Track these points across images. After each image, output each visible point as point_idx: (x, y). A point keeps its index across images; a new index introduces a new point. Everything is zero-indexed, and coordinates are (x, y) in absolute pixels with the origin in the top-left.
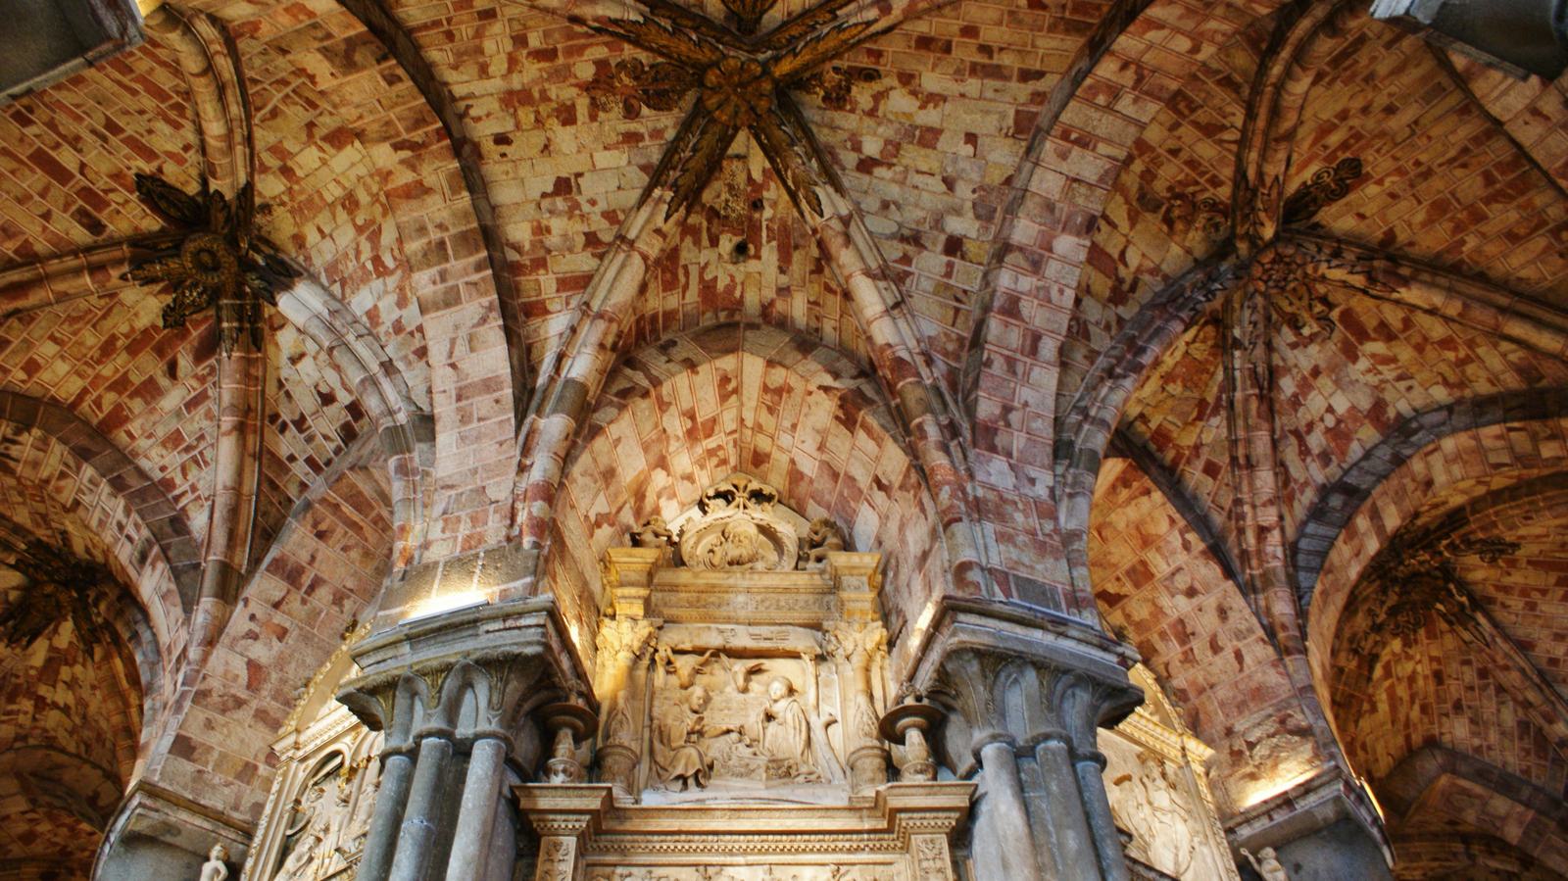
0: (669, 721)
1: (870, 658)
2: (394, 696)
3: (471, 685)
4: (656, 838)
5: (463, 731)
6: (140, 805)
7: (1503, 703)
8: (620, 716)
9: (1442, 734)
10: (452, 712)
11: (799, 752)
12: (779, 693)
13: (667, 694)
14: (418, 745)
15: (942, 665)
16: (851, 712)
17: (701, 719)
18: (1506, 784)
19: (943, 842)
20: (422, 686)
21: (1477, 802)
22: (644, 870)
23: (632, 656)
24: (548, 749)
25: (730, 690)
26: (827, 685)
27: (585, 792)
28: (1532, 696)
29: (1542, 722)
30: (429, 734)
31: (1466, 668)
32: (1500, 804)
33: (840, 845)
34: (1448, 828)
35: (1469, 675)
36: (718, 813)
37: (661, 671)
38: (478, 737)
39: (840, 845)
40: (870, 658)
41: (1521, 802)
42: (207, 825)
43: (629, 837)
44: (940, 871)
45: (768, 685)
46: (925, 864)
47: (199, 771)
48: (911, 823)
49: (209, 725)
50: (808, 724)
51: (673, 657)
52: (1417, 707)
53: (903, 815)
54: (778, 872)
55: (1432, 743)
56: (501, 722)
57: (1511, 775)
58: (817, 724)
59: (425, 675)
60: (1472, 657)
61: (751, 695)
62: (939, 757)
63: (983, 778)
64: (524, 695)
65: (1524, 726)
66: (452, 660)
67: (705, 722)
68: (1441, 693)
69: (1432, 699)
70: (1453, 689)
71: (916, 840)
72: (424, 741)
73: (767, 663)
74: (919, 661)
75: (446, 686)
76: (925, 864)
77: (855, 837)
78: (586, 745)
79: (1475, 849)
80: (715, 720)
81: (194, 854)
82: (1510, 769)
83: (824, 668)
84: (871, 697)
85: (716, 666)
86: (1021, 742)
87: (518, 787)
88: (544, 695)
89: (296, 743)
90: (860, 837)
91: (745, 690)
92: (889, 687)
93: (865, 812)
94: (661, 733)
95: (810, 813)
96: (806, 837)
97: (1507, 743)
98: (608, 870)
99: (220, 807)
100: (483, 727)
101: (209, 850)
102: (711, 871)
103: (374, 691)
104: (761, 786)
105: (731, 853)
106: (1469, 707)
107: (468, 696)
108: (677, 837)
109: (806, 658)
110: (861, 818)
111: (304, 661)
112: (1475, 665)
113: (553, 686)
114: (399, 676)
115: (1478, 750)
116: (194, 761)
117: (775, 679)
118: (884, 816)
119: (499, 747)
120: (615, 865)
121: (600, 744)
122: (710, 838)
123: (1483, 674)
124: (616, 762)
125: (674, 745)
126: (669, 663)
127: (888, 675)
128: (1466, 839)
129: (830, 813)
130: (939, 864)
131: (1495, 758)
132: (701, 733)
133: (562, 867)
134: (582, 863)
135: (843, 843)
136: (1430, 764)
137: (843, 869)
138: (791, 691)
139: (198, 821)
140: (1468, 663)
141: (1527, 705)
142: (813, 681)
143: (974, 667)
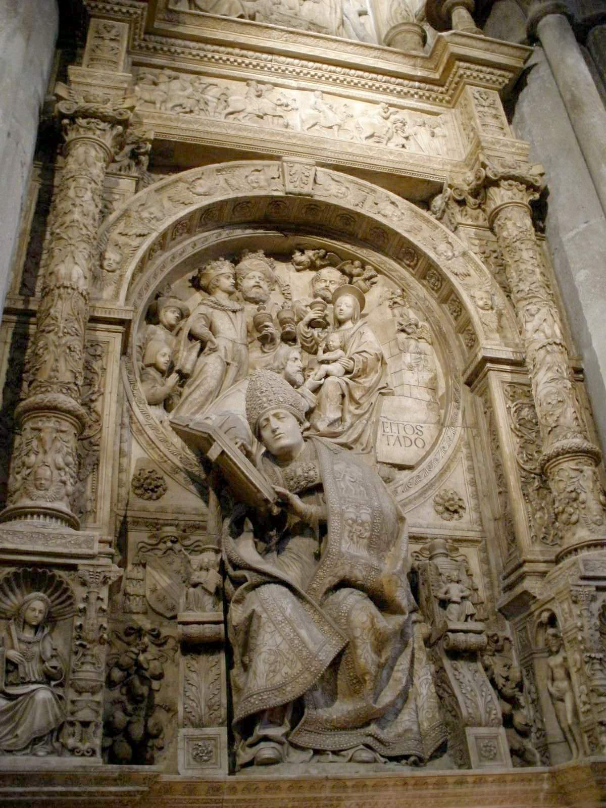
4: (209, 47)
19: (496, 97)
22: (192, 76)
33: (392, 87)
36: (275, 33)
39: (392, 87)
43: (179, 42)
48: (468, 73)
53: (461, 64)
71: (471, 91)
77: (406, 82)
90: (411, 83)
93: (419, 61)
95: (367, 51)
105: (283, 74)
108: (230, 50)
110: (414, 66)
122: (265, 56)
135: (393, 84)
137: (392, 109)
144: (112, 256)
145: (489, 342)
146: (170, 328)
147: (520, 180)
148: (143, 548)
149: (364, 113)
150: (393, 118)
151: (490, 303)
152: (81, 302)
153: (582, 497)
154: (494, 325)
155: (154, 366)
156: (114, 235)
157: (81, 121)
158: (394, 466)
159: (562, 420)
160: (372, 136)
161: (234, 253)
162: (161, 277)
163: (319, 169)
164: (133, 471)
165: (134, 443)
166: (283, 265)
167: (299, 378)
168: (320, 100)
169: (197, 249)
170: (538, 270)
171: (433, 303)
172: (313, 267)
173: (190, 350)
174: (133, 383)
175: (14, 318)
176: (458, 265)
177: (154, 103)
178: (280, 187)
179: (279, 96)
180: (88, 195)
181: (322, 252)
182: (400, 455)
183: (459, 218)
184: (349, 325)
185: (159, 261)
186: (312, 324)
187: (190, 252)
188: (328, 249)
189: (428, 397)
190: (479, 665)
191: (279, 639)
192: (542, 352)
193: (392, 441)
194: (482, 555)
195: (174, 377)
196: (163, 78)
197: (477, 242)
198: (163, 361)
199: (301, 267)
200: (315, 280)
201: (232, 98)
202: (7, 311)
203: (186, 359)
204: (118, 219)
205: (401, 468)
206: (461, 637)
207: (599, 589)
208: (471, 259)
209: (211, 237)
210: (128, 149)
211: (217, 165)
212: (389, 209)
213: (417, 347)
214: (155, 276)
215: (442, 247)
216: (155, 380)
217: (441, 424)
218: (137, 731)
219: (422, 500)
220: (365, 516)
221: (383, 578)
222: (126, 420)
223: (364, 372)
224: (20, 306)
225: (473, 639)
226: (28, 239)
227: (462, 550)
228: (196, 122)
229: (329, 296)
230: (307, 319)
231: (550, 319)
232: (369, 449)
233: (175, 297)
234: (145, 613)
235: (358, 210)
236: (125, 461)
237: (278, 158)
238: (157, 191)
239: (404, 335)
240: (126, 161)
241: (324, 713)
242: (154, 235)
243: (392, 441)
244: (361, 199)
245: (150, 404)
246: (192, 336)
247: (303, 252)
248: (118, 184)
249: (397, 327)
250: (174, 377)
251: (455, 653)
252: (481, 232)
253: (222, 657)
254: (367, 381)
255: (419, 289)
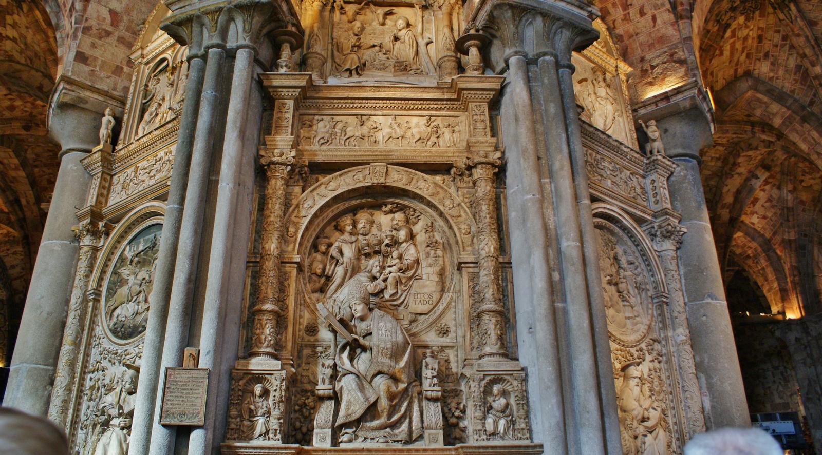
0: (342, 40)
1: (452, 8)
2: (192, 26)
3: (233, 19)
4: (335, 101)
5: (231, 44)
6: (64, 88)
7: (791, 54)
8: (315, 37)
9: (754, 70)
10: (224, 34)
11: (412, 57)
12: (401, 26)
13: (341, 25)
14: (207, 52)
15: (491, 12)
16: (441, 37)
17: (360, 39)
18: (780, 97)
19: (485, 106)
20: (207, 20)
21: (764, 105)
22: (329, 117)
23: (321, 4)
24: (277, 54)
25: (375, 23)
26: (428, 22)
27: (297, 77)
28: (808, 51)
29: (809, 65)
30: (212, 47)
31: (776, 35)
32: (775, 107)
33: (432, 106)
34: (745, 118)
35: (777, 38)
36: (368, 88)
37: (337, 13)
38: (239, 47)
39: (432, 106)
40: (452, 8)
41: (786, 107)
42: (101, 99)
43: (321, 101)
44: (483, 121)
45: (396, 21)
46: (475, 117)
47: (92, 70)
49: (93, 46)
50: (417, 43)
51: (344, 5)
52: (744, 55)
54: (399, 119)
55: (748, 74)
56: (251, 39)
57: (785, 93)
58: (422, 43)
59: (207, 14)
60: (781, 29)
61: (387, 26)
62: (486, 63)
63: (509, 74)
64: (262, 24)
65: (798, 67)
66: (222, 5)
67: (362, 40)
68: (760, 48)
69: (754, 51)
70: (766, 45)
72: (210, 50)
73: (396, 10)
74: (479, 10)
75: (219, 20)
76: (475, 117)
78: (297, 52)
79: (757, 129)
80: (367, 40)
81: (97, 113)
82: (785, 90)
83: (427, 14)
84: (452, 30)
85: (367, 10)
86: (530, 56)
87: (262, 74)
88: (273, 25)
89: (142, 54)
91: (383, 24)
92: (461, 24)
94: (338, 46)
95: (416, 90)
96: (414, 102)
97: (787, 76)
98: (311, 117)
99: (106, 89)
100: (241, 42)
101: (104, 111)
102: (364, 118)
103: (180, 23)
104: (391, 75)
105: (375, 109)
106: (773, 56)
107: (232, 26)
108: (346, 101)
109: (417, 7)
111: (141, 10)
112: (782, 33)
113: (279, 20)
114: (193, 15)
115: (771, 79)
116: (88, 65)
117: (399, 18)
118: (455, 92)
119: (251, 53)
120: (314, 115)
121: (305, 52)
123: (785, 38)
124: (314, 61)
125: (345, 53)
126: (342, 8)
127: (462, 18)
128: (753, 124)
129: (427, 90)
130: (482, 117)
131: (778, 83)
132: (359, 47)
133: (287, 115)
134: (297, 114)
136: (744, 85)
137: (433, 119)
138: (408, 25)
139: (96, 96)
140: (778, 31)
141: (804, 56)
142: (421, 20)
143: (509, 14)
144: (292, 230)
145: (465, 253)
146: (324, 253)
147: (488, 163)
148: (308, 357)
149: (417, 125)
150: (432, 124)
151: (468, 231)
152: (276, 261)
153: (489, 333)
154: (469, 243)
155: (316, 274)
156: (293, 218)
157: (272, 166)
158: (417, 314)
159: (487, 295)
160: (420, 139)
161: (354, 211)
162: (318, 230)
163: (389, 166)
164: (305, 324)
165: (306, 312)
166: (378, 212)
167: (378, 275)
168: (393, 122)
169: (334, 213)
170: (488, 216)
171: (446, 229)
172: (391, 212)
173: (331, 265)
174: (305, 284)
175: (251, 264)
176: (454, 212)
177: (310, 138)
178: (369, 180)
179: (372, 123)
180: (278, 205)
181: (395, 205)
182: (421, 308)
183: (459, 184)
184: (404, 245)
185: (316, 223)
186: (387, 245)
187: (331, 215)
188: (397, 204)
189: (437, 279)
190: (439, 404)
191: (350, 397)
192: (483, 261)
193: (417, 302)
194: (455, 353)
195: (323, 280)
196: (315, 122)
197: (468, 196)
198: (319, 271)
199: (386, 213)
200: (393, 219)
201: (348, 129)
202: (248, 262)
203: (329, 269)
204: (294, 210)
205: (421, 314)
206: (429, 394)
207: (485, 375)
208: (463, 208)
209: (341, 207)
210: (297, 170)
211: (339, 173)
212: (422, 184)
213: (435, 254)
214: (315, 230)
215: (448, 202)
216: (315, 281)
217: (443, 291)
218: (304, 430)
219: (429, 329)
220: (389, 346)
221: (396, 371)
222: (302, 302)
223: (408, 269)
224: (253, 260)
225: (434, 394)
226: (255, 225)
227: (447, 351)
228: (328, 151)
229: (397, 227)
230: (385, 243)
231: (490, 243)
232: (407, 307)
233: (326, 237)
234: (309, 383)
235: (408, 188)
236: (302, 320)
237: (369, 164)
238: (312, 191)
239: (429, 248)
240: (297, 177)
241: (368, 424)
242: (310, 216)
243: (417, 302)
244: (410, 180)
245: (313, 292)
246: (332, 257)
247: (386, 206)
248: (293, 190)
249: (426, 245)
250: (323, 280)
251: (429, 399)
252: (470, 190)
253: (333, 402)
254: (410, 273)
255: (440, 222)
